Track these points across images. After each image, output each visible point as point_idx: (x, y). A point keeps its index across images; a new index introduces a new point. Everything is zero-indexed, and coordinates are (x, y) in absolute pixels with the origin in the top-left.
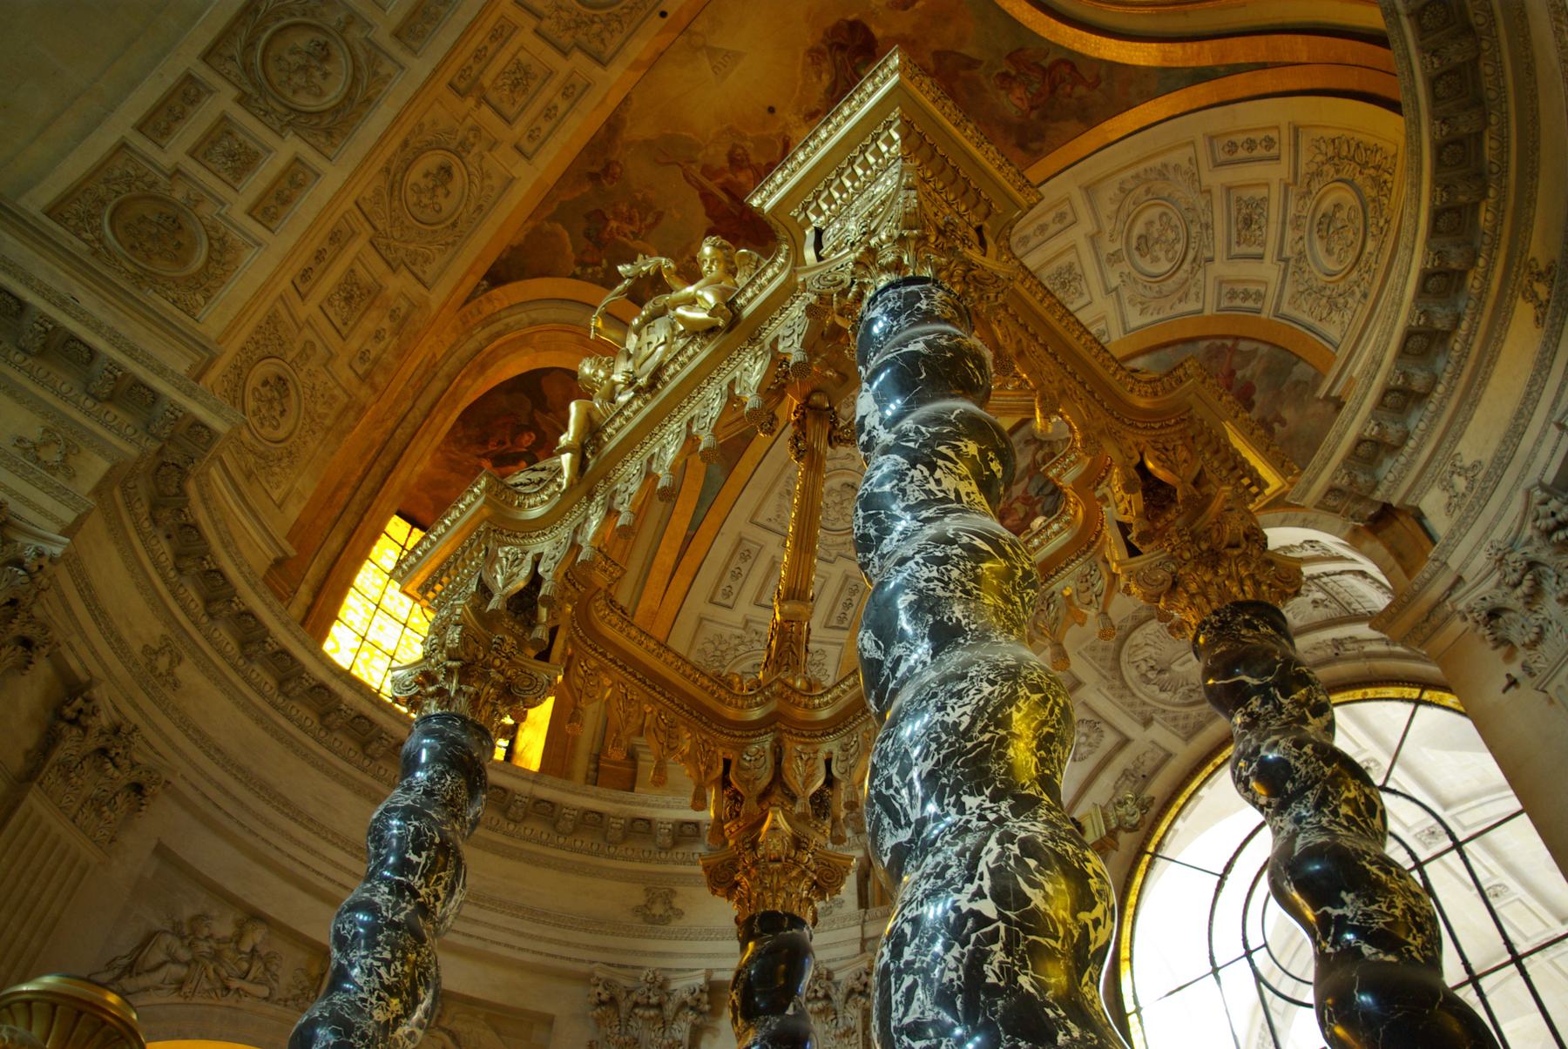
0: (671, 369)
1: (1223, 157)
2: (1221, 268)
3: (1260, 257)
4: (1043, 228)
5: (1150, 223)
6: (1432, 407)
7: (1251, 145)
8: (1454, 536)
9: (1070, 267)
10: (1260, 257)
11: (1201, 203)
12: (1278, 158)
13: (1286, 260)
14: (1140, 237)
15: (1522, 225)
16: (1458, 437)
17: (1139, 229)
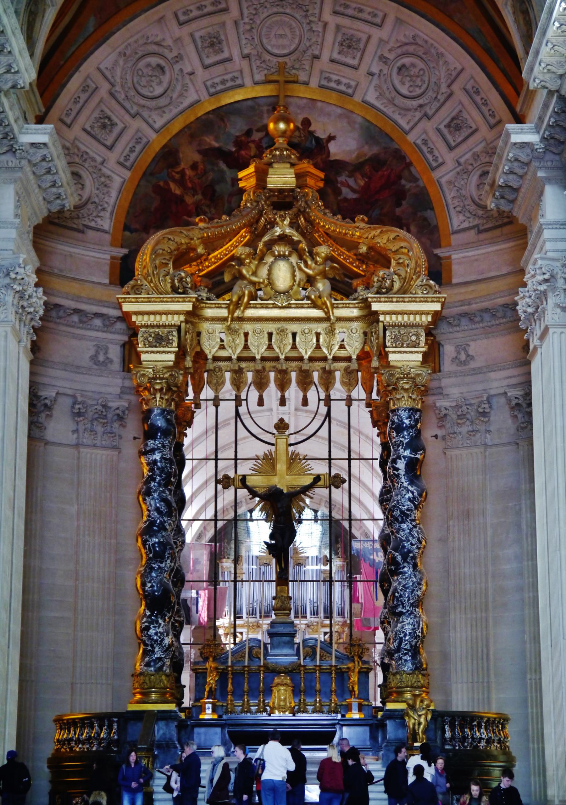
0: (293, 306)
1: (469, 87)
2: (429, 126)
3: (451, 148)
4: (361, 11)
5: (413, 65)
6: (474, 326)
7: (486, 104)
8: (450, 375)
9: (359, 40)
10: (451, 148)
11: (444, 88)
12: (492, 127)
13: (459, 164)
14: (404, 66)
16: (473, 340)
17: (406, 61)
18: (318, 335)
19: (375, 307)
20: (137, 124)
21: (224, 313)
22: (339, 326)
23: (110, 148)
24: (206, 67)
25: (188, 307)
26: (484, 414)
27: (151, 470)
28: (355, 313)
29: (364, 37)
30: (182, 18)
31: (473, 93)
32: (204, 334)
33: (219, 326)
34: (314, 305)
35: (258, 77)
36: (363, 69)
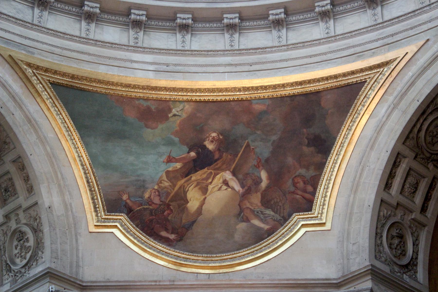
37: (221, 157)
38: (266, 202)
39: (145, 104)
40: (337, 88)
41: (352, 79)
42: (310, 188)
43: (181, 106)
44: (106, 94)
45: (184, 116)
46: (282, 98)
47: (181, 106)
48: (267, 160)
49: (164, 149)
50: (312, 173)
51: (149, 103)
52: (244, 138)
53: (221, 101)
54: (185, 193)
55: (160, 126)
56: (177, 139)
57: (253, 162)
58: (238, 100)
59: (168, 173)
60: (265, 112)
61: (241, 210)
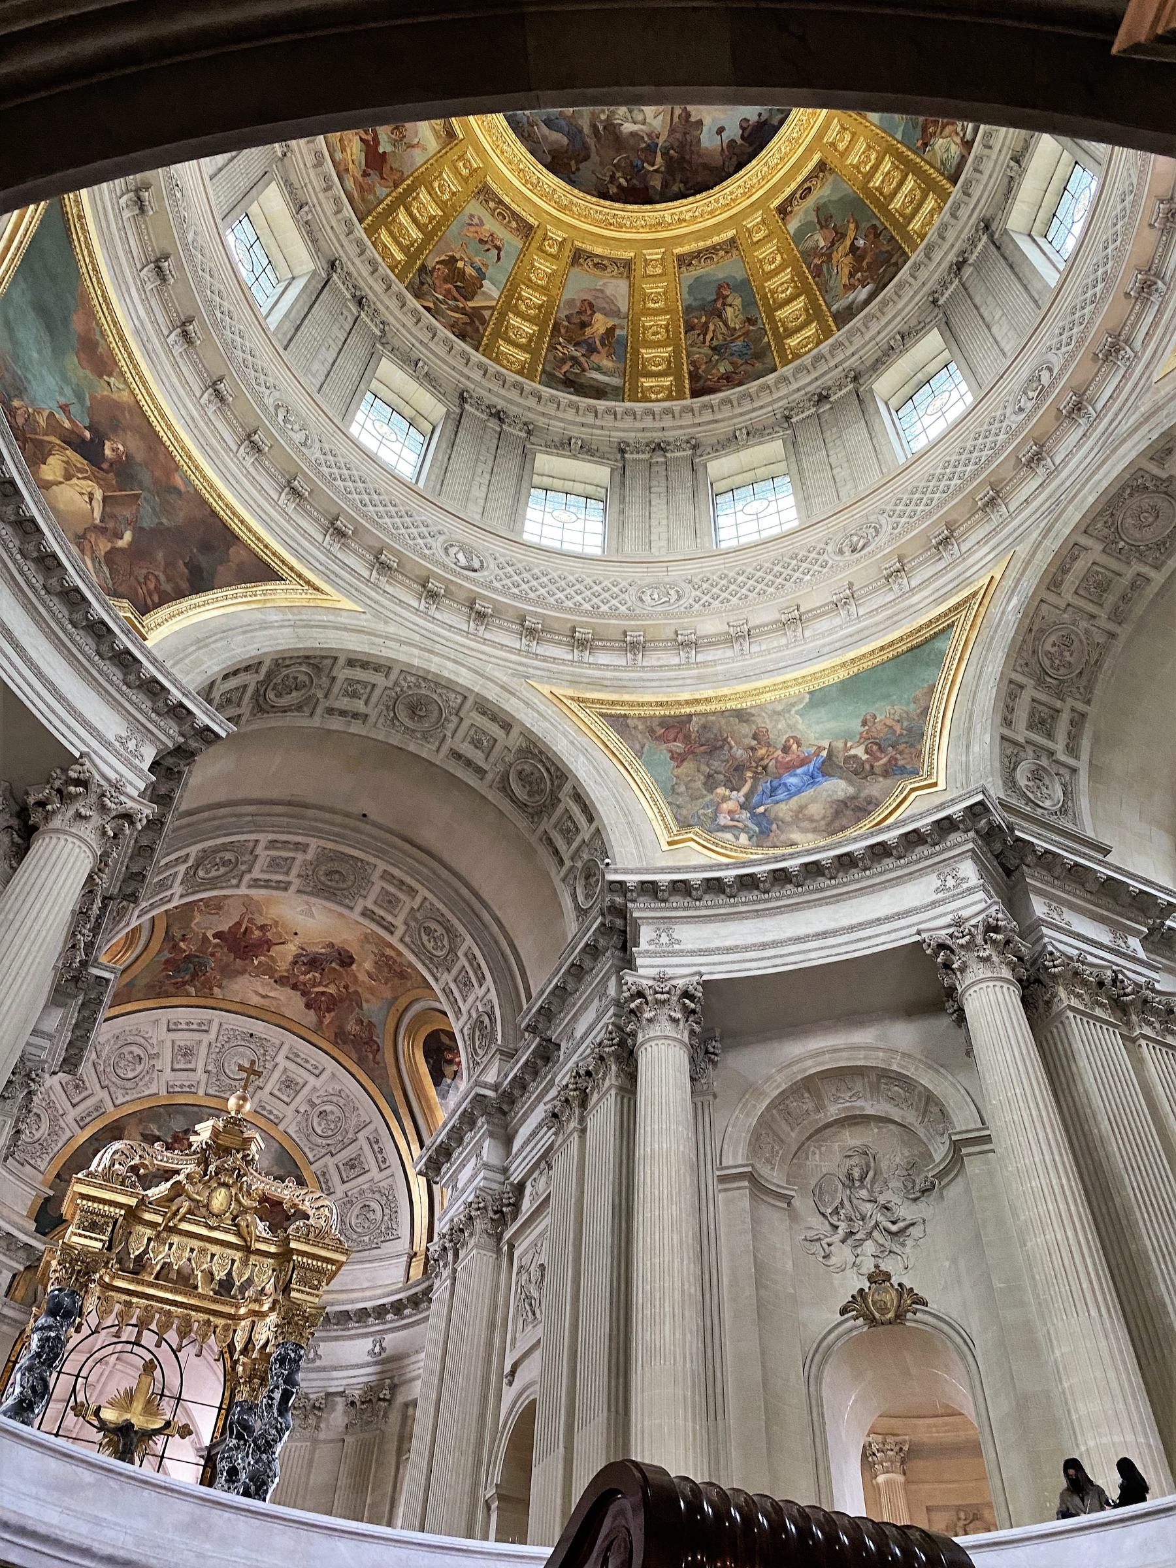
15: (392, 1330)
18: (233, 1261)
19: (293, 1245)
20: (104, 1094)
21: (159, 1219)
22: (253, 1259)
23: (74, 1106)
24: (173, 1070)
25: (133, 1202)
26: (319, 1409)
27: (41, 1347)
28: (273, 1249)
29: (301, 1081)
30: (172, 1027)
31: (374, 1142)
32: (133, 1237)
33: (149, 1232)
34: (239, 1234)
35: (210, 1091)
36: (293, 1106)
37: (107, 472)
38: (111, 558)
39: (98, 337)
40: (256, 555)
41: (275, 565)
42: (156, 598)
43: (121, 386)
44: (79, 276)
45: (115, 396)
46: (206, 502)
47: (121, 386)
48: (142, 529)
49: (68, 391)
50: (168, 587)
51: (102, 341)
52: (141, 485)
53: (156, 434)
54: (50, 454)
55: (88, 372)
56: (88, 403)
57: (127, 512)
58: (170, 453)
59: (51, 415)
60: (179, 492)
61: (83, 537)
